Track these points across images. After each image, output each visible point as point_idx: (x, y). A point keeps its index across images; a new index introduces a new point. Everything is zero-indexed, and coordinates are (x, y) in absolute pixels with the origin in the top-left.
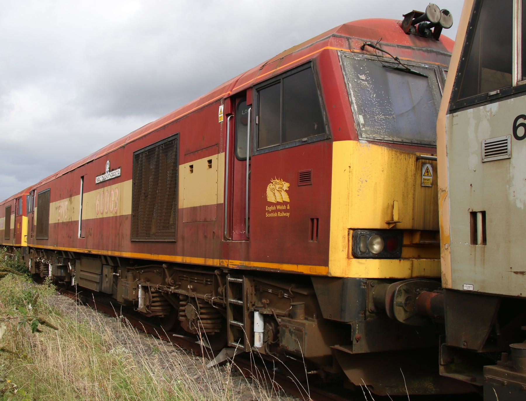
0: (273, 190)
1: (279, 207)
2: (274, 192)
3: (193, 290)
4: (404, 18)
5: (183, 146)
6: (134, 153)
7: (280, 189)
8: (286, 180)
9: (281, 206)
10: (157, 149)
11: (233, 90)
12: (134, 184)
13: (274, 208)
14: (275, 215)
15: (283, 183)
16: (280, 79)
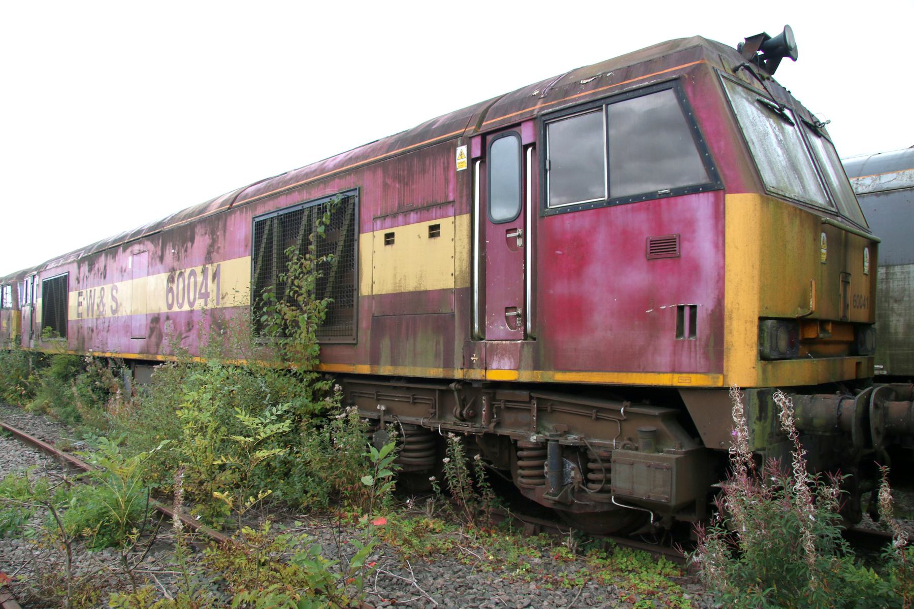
3: (387, 412)
4: (744, 41)
5: (369, 207)
6: (253, 218)
11: (484, 124)
12: (255, 260)
16: (602, 106)
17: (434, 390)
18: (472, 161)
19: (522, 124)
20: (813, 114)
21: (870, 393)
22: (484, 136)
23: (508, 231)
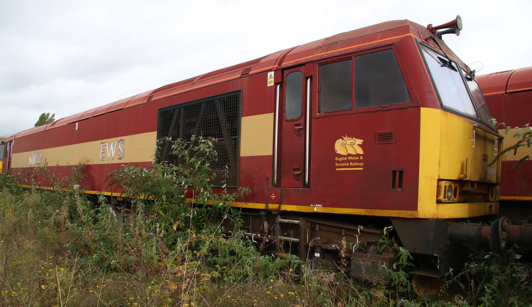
0: (344, 145)
1: (350, 158)
2: (345, 146)
7: (352, 144)
8: (358, 137)
9: (353, 157)
10: (177, 111)
11: (283, 64)
13: (346, 159)
14: (347, 164)
15: (357, 140)
17: (249, 215)
18: (276, 84)
19: (306, 64)
20: (467, 65)
21: (498, 222)
22: (283, 70)
23: (296, 125)
